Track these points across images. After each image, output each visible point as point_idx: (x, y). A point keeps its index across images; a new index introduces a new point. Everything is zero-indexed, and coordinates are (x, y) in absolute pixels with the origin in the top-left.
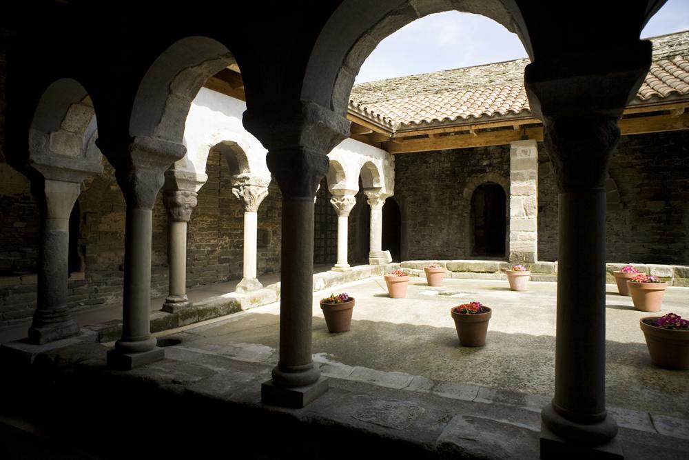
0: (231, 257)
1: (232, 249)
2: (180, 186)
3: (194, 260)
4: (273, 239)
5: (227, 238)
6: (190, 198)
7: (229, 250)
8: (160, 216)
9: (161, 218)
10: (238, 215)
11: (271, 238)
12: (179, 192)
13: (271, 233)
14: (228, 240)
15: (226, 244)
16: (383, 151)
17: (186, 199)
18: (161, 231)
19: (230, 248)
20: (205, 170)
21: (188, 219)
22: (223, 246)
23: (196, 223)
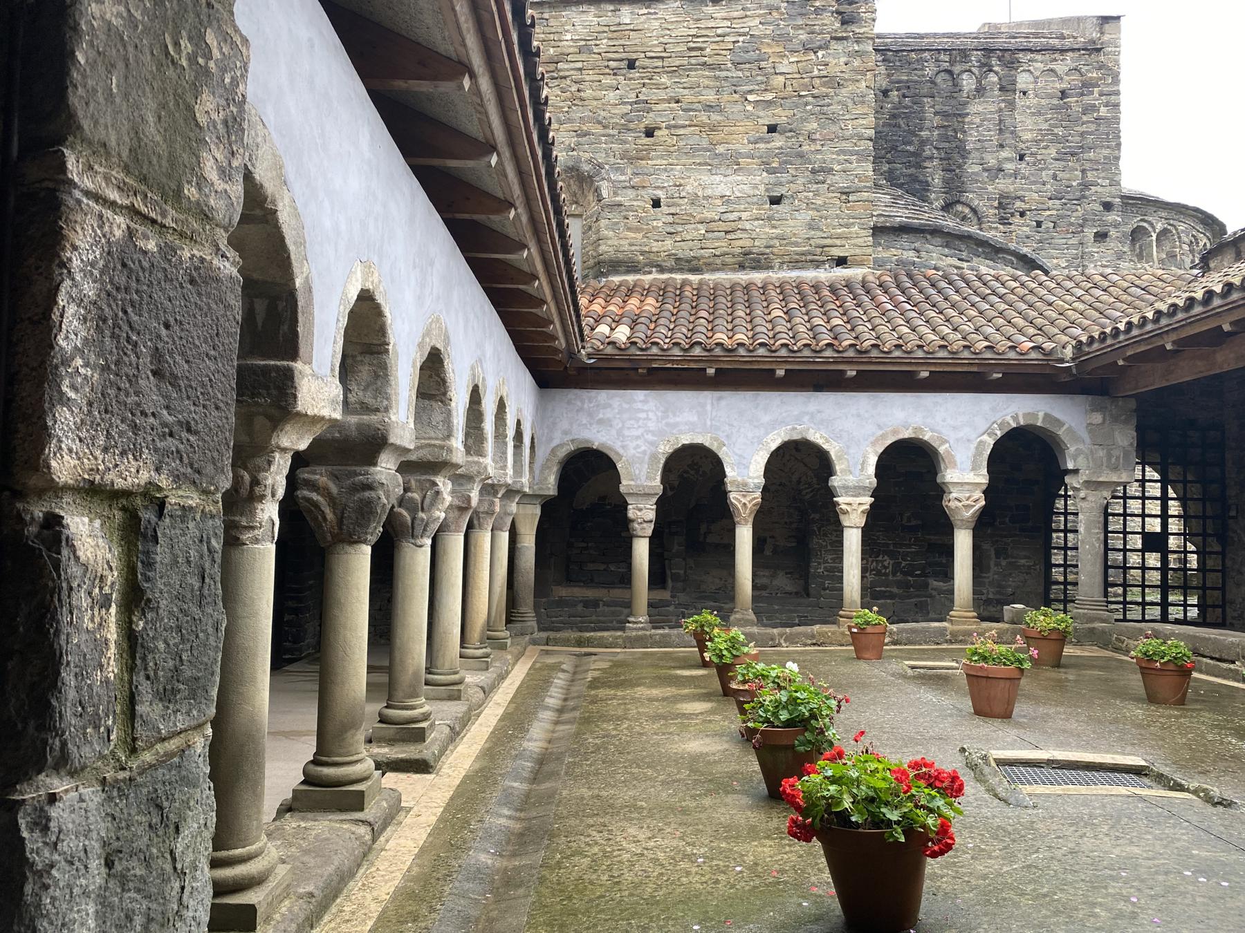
0: (895, 590)
1: (899, 576)
2: (629, 500)
3: (825, 589)
4: (997, 565)
5: (886, 557)
6: (644, 511)
7: (890, 577)
8: (791, 523)
9: (794, 526)
10: (909, 520)
11: (992, 564)
12: (630, 507)
13: (993, 553)
14: (888, 561)
15: (886, 568)
16: (1080, 399)
17: (639, 514)
18: (794, 544)
19: (894, 574)
20: (659, 478)
21: (649, 532)
22: (880, 571)
23: (825, 535)
